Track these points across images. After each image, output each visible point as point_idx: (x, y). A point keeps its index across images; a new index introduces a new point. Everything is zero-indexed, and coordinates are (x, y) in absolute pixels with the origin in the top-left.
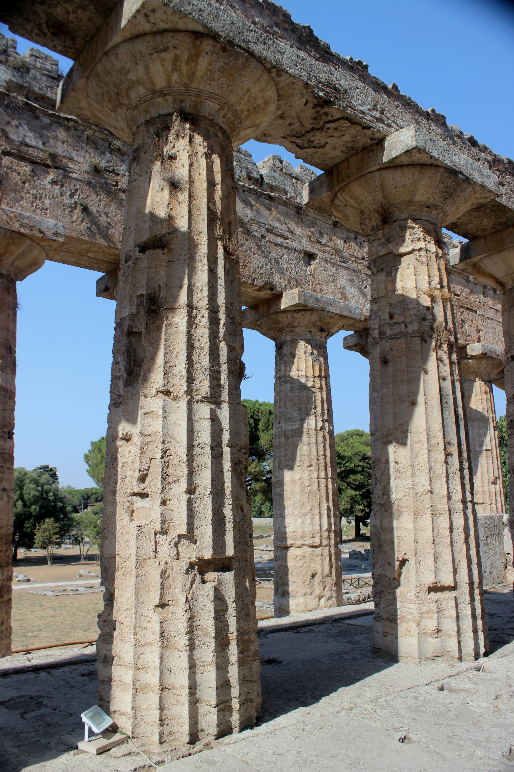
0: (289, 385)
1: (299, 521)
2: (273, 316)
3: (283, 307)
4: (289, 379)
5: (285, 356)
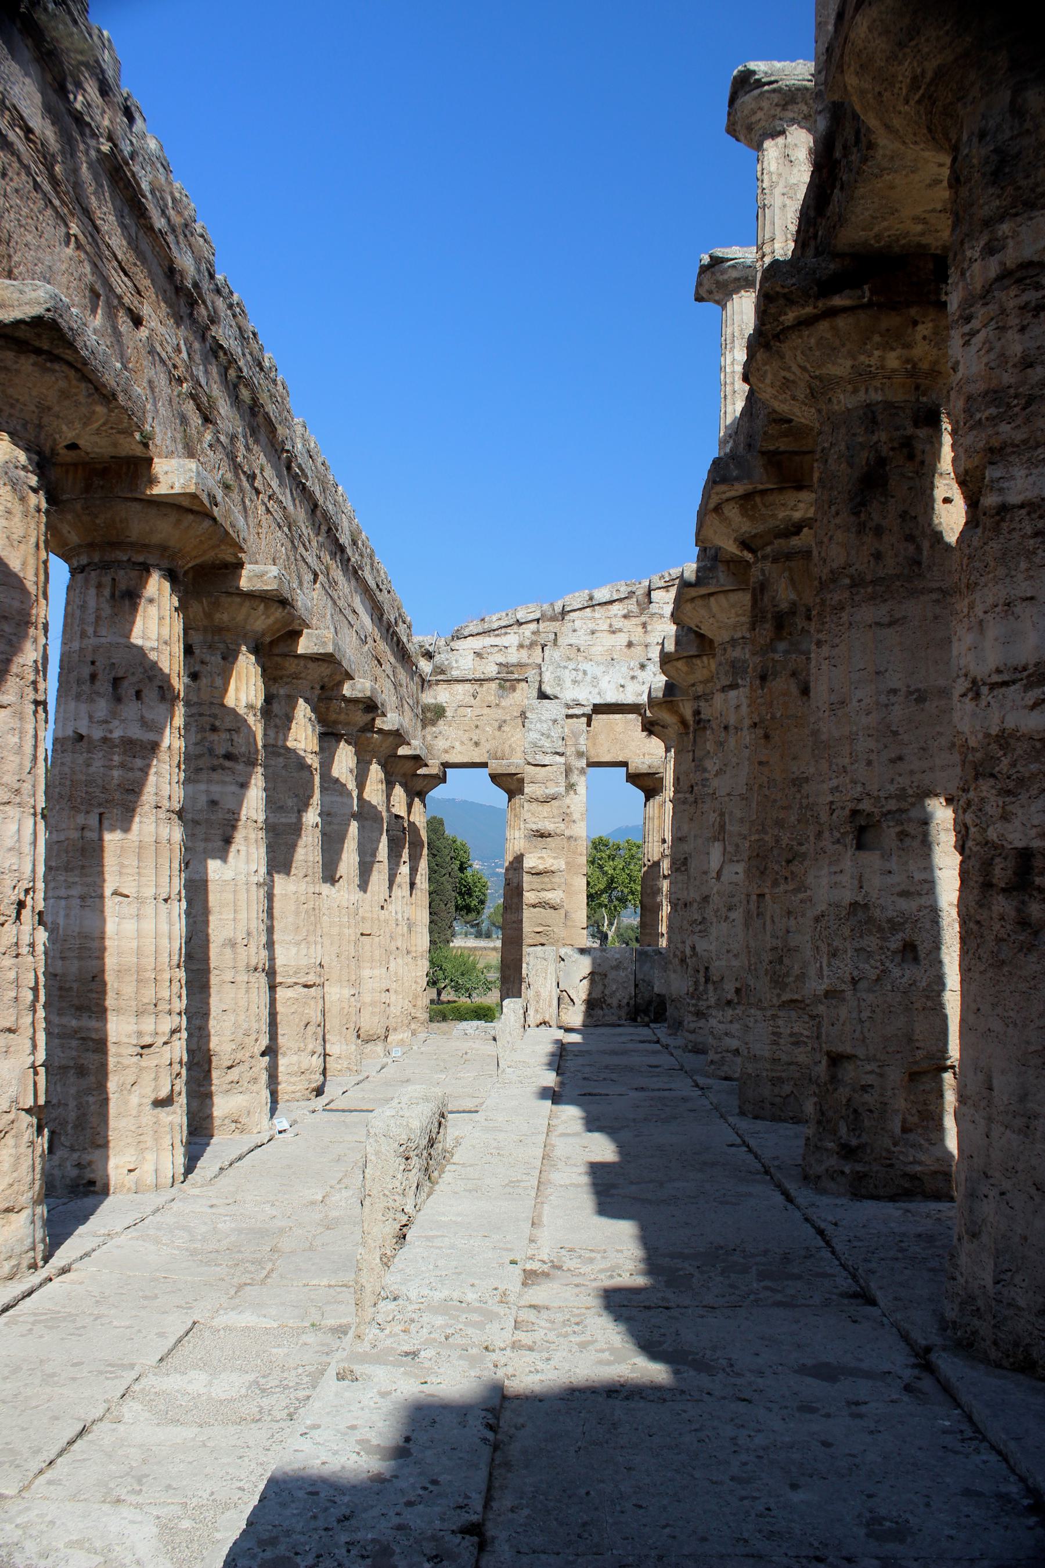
0: (281, 760)
1: (294, 950)
2: (279, 659)
3: (300, 651)
5: (276, 716)
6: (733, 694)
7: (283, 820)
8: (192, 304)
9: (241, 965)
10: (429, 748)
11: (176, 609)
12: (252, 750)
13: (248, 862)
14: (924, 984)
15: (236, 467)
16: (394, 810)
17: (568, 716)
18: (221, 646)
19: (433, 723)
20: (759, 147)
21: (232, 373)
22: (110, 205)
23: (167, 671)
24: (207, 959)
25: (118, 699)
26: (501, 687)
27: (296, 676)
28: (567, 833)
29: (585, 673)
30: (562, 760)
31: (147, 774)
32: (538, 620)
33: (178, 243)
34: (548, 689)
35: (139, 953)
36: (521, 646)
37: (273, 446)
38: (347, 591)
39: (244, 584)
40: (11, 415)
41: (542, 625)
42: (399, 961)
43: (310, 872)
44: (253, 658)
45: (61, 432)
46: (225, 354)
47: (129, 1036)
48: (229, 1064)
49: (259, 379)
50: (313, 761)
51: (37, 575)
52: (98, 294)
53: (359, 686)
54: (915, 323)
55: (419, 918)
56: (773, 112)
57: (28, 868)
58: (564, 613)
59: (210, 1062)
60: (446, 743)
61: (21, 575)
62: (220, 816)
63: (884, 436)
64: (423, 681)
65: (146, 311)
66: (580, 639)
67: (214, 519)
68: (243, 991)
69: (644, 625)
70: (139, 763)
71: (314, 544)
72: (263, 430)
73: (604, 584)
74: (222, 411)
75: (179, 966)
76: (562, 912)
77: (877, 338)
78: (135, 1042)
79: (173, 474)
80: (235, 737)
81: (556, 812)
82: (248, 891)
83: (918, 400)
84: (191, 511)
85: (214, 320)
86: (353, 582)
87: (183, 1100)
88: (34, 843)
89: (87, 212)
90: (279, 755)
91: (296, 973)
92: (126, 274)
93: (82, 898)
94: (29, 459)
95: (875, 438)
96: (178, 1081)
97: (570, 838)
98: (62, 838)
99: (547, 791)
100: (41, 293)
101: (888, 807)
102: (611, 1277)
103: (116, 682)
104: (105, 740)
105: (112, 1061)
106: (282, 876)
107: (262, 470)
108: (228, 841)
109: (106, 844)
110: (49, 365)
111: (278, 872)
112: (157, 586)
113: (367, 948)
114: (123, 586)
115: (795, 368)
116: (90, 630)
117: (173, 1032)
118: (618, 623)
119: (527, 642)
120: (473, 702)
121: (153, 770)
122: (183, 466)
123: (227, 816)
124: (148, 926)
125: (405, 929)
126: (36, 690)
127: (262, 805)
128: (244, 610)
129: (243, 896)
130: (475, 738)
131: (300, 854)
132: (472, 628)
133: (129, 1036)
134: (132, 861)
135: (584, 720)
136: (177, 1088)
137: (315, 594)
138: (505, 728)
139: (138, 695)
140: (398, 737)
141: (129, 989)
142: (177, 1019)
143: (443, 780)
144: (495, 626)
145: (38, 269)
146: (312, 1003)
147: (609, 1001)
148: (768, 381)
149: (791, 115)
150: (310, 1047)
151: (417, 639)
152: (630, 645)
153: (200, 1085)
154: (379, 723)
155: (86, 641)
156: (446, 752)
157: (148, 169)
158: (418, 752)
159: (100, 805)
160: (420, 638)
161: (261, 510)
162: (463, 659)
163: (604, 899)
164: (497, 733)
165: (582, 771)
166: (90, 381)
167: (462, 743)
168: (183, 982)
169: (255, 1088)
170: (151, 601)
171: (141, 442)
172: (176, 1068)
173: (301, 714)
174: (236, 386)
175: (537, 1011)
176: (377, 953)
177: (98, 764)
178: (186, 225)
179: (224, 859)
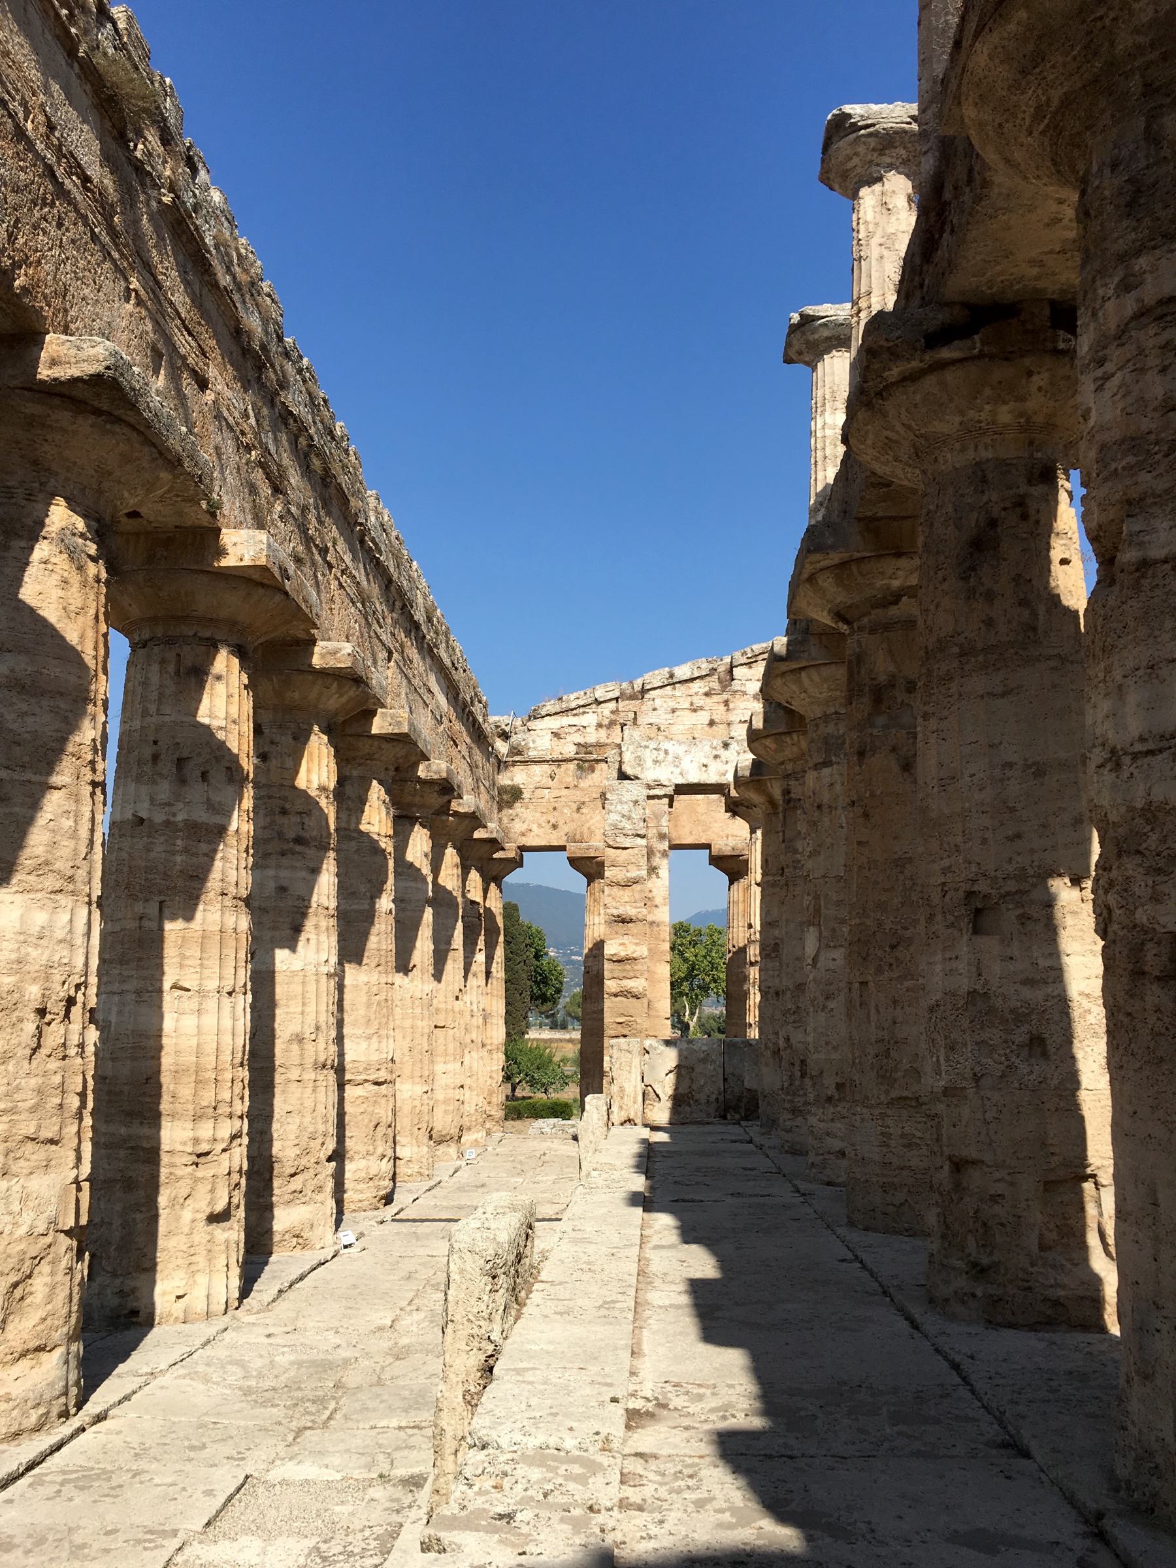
0: (353, 843)
3: (375, 730)
4: (355, 835)
5: (349, 798)
6: (826, 771)
7: (356, 907)
8: (260, 367)
9: (309, 1062)
10: (506, 831)
11: (246, 687)
12: (324, 834)
13: (318, 951)
14: (1056, 1082)
15: (308, 540)
16: (470, 896)
17: (650, 797)
18: (292, 725)
19: (510, 805)
20: (855, 196)
21: (303, 441)
22: (171, 259)
23: (235, 751)
24: (272, 1056)
25: (183, 781)
26: (579, 767)
27: (370, 757)
28: (650, 918)
29: (666, 752)
30: (643, 842)
31: (213, 859)
32: (617, 699)
33: (244, 302)
34: (628, 770)
35: (199, 1051)
36: (600, 726)
37: (345, 518)
38: (422, 669)
39: (317, 661)
40: (67, 479)
41: (621, 704)
42: (474, 1054)
43: (383, 961)
44: (325, 738)
45: (122, 498)
46: (295, 421)
47: (185, 1144)
48: (293, 1171)
49: (330, 449)
50: (387, 845)
51: (96, 649)
52: (161, 353)
53: (434, 767)
54: (1030, 374)
55: (494, 1009)
56: (869, 157)
57: (79, 962)
58: (644, 691)
59: (271, 1169)
60: (525, 825)
61: (79, 648)
62: (290, 903)
63: (995, 497)
64: (499, 762)
65: (212, 372)
66: (661, 718)
67: (286, 593)
68: (310, 1090)
69: (726, 703)
70: (204, 847)
71: (389, 621)
72: (335, 502)
73: (685, 662)
74: (292, 481)
75: (242, 1065)
76: (645, 1001)
77: (988, 392)
78: (190, 1150)
79: (243, 546)
80: (306, 820)
81: (637, 896)
82: (317, 981)
83: (1032, 455)
84: (262, 585)
85: (283, 384)
86: (428, 660)
87: (241, 1213)
88: (88, 934)
89: (147, 268)
90: (353, 839)
91: (366, 1069)
92: (190, 334)
93: (138, 993)
94: (87, 526)
95: (985, 498)
96: (237, 1192)
97: (652, 923)
98: (118, 928)
99: (628, 875)
100: (100, 350)
101: (1007, 889)
102: (724, 1418)
103: (181, 762)
104: (167, 823)
105: (164, 1172)
106: (353, 965)
107: (335, 543)
108: (297, 929)
109: (166, 934)
110: (108, 426)
111: (349, 962)
112: (225, 663)
113: (441, 1040)
114: (188, 662)
115: (899, 427)
116: (153, 708)
117: (233, 1137)
118: (699, 701)
119: (606, 722)
120: (550, 783)
121: (219, 855)
122: (253, 537)
123: (296, 903)
124: (209, 1021)
125: (481, 1020)
126: (94, 770)
127: (333, 892)
128: (315, 691)
129: (312, 987)
130: (553, 821)
131: (373, 942)
132: (550, 707)
133: (185, 1144)
134: (194, 951)
135: (666, 801)
136: (235, 1201)
137: (389, 673)
138: (583, 810)
139: (204, 776)
140: (475, 819)
141: (186, 1092)
142: (238, 1123)
143: (520, 864)
144: (573, 705)
145: (96, 325)
146: (383, 1101)
147: (697, 1096)
148: (869, 442)
149: (888, 160)
150: (380, 1150)
151: (494, 720)
152: (712, 723)
153: (259, 1196)
154: (455, 805)
155: (148, 719)
156: (523, 835)
157: (212, 222)
158: (494, 835)
159: (160, 892)
160: (496, 718)
161: (334, 585)
162: (540, 739)
163: (685, 987)
164: (576, 815)
165: (664, 854)
166: (154, 445)
167: (540, 826)
168: (246, 1082)
169: (320, 1197)
170: (219, 678)
171: (208, 512)
172: (235, 1177)
173: (375, 796)
174: (306, 455)
175: (621, 1108)
176: (451, 1046)
177: (159, 848)
178: (253, 284)
179: (293, 949)
